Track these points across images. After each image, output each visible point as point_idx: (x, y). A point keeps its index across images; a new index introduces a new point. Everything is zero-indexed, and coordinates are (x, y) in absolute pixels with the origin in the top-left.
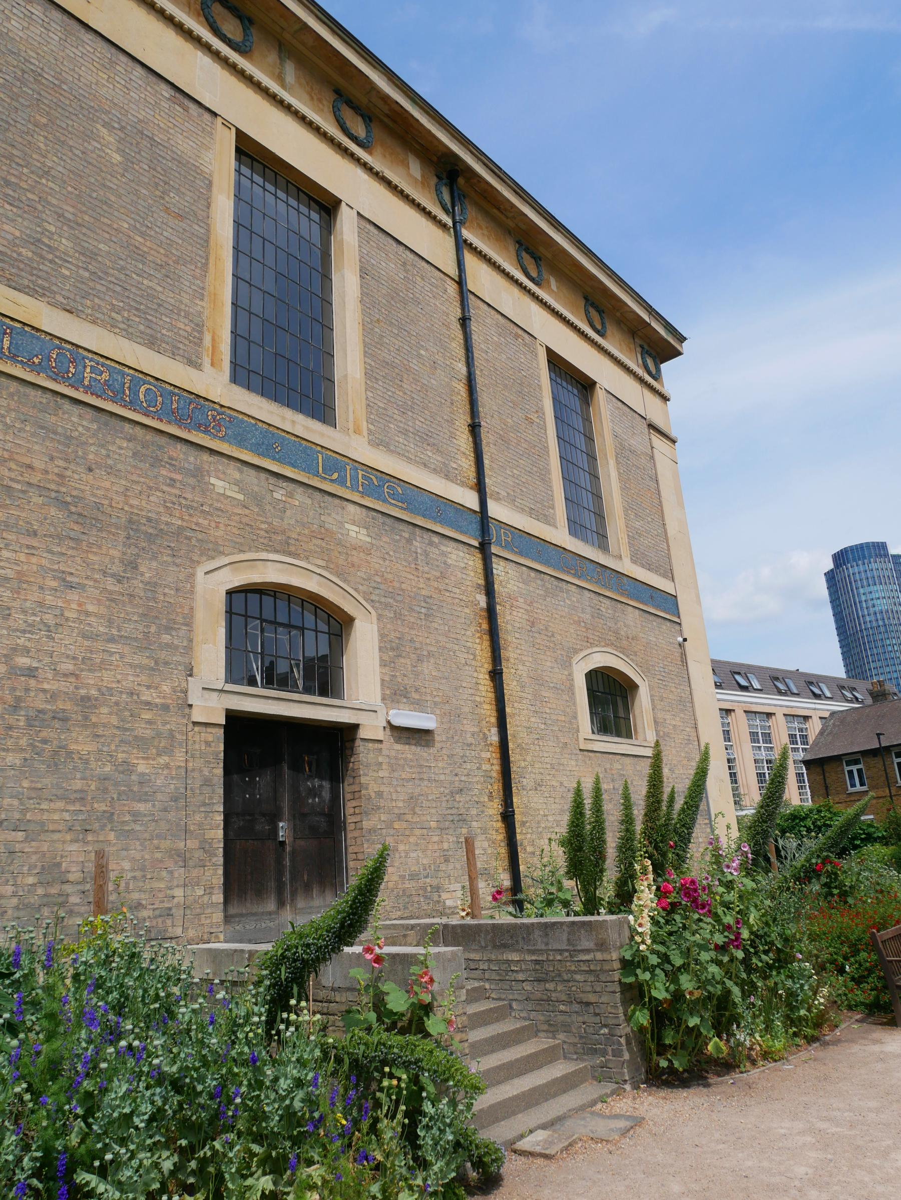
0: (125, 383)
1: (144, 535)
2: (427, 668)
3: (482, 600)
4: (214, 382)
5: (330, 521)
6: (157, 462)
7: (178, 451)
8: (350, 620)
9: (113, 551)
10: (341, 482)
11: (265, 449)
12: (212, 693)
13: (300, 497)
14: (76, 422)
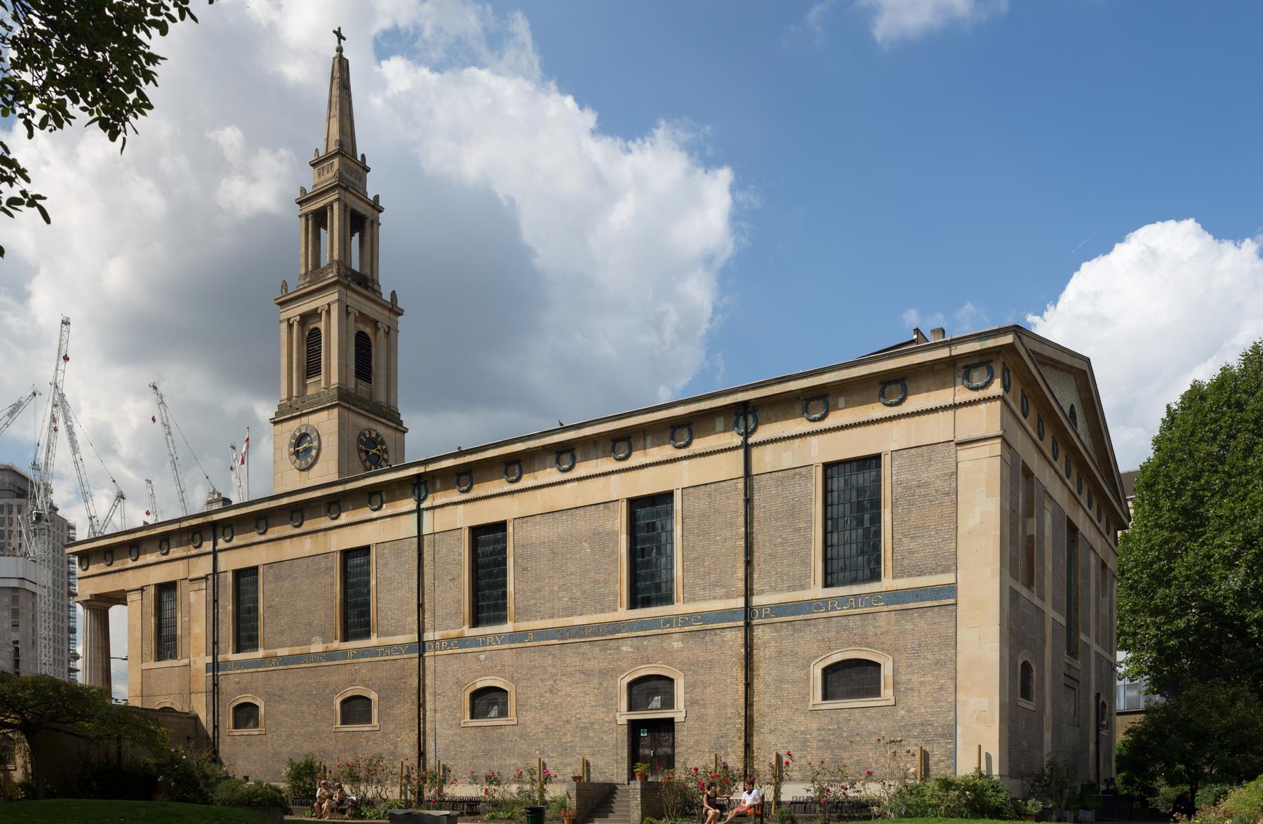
0: (597, 629)
1: (604, 673)
2: (709, 690)
4: (623, 613)
5: (665, 645)
6: (606, 649)
7: (611, 644)
8: (672, 680)
9: (596, 681)
10: (671, 627)
11: (641, 628)
12: (624, 716)
13: (654, 640)
14: (585, 647)
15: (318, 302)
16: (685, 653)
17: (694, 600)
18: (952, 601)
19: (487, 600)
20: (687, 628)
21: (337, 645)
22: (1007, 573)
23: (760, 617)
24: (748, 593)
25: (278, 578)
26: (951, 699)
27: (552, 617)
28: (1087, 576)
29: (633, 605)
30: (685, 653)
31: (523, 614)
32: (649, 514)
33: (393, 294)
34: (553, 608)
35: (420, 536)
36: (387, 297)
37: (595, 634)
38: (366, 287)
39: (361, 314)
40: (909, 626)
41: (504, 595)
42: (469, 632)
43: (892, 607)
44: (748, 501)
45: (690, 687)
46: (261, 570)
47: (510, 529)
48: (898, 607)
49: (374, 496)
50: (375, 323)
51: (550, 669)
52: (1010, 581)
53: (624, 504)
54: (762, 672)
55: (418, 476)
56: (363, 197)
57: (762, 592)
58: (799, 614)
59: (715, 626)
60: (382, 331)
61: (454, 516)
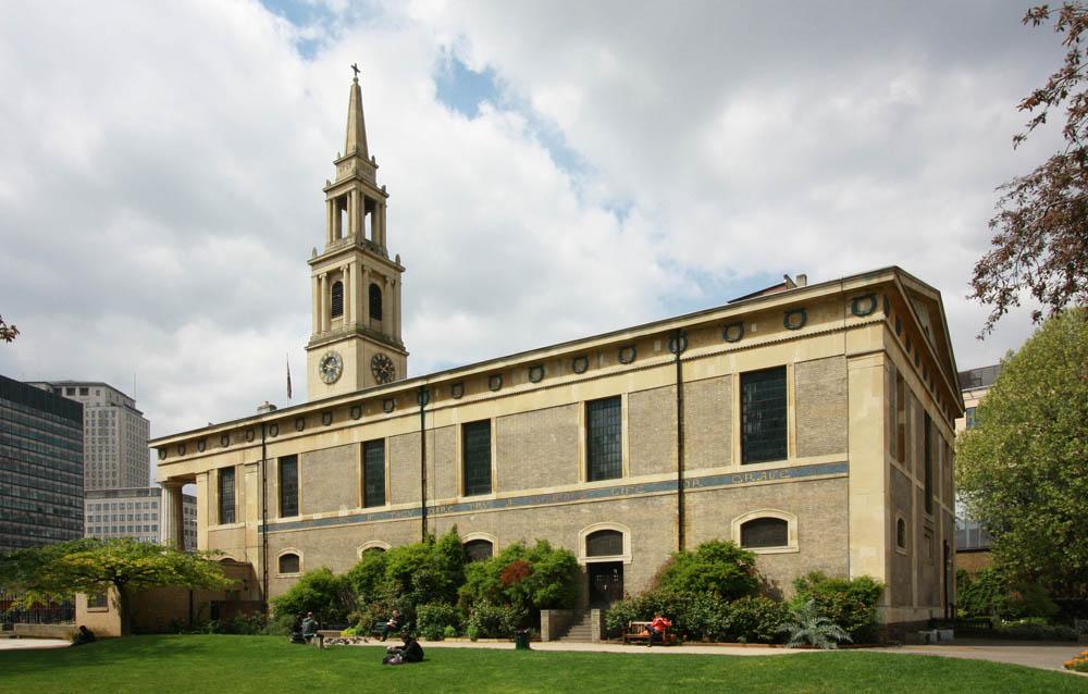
0: (562, 497)
2: (650, 541)
3: (677, 512)
8: (621, 534)
9: (561, 536)
10: (620, 494)
11: (596, 495)
13: (606, 504)
14: (553, 510)
15: (341, 263)
16: (632, 514)
17: (638, 475)
18: (845, 474)
19: (476, 477)
20: (633, 496)
21: (360, 510)
22: (888, 453)
23: (691, 487)
24: (681, 469)
25: (313, 462)
26: (845, 548)
27: (526, 488)
28: (937, 453)
29: (589, 479)
30: (632, 514)
31: (504, 486)
32: (602, 411)
33: (398, 257)
34: (527, 482)
35: (423, 431)
36: (392, 258)
37: (560, 500)
38: (377, 252)
39: (374, 271)
40: (810, 493)
41: (490, 471)
42: (462, 500)
43: (796, 479)
44: (680, 402)
45: (635, 539)
46: (299, 457)
47: (493, 425)
48: (801, 479)
49: (387, 403)
50: (384, 278)
51: (526, 527)
52: (890, 458)
53: (583, 405)
54: (693, 527)
55: (422, 387)
56: (373, 187)
57: (692, 468)
58: (722, 484)
59: (655, 493)
60: (389, 285)
61: (450, 416)
